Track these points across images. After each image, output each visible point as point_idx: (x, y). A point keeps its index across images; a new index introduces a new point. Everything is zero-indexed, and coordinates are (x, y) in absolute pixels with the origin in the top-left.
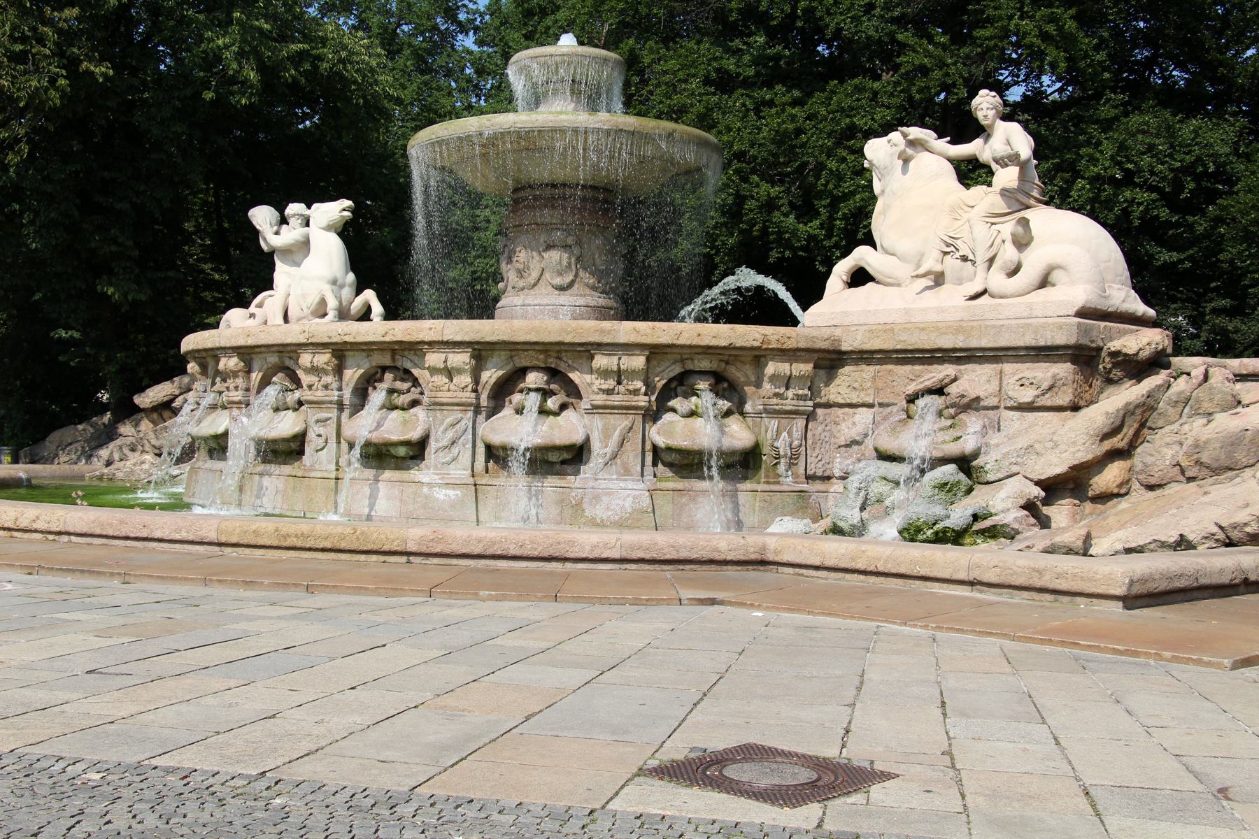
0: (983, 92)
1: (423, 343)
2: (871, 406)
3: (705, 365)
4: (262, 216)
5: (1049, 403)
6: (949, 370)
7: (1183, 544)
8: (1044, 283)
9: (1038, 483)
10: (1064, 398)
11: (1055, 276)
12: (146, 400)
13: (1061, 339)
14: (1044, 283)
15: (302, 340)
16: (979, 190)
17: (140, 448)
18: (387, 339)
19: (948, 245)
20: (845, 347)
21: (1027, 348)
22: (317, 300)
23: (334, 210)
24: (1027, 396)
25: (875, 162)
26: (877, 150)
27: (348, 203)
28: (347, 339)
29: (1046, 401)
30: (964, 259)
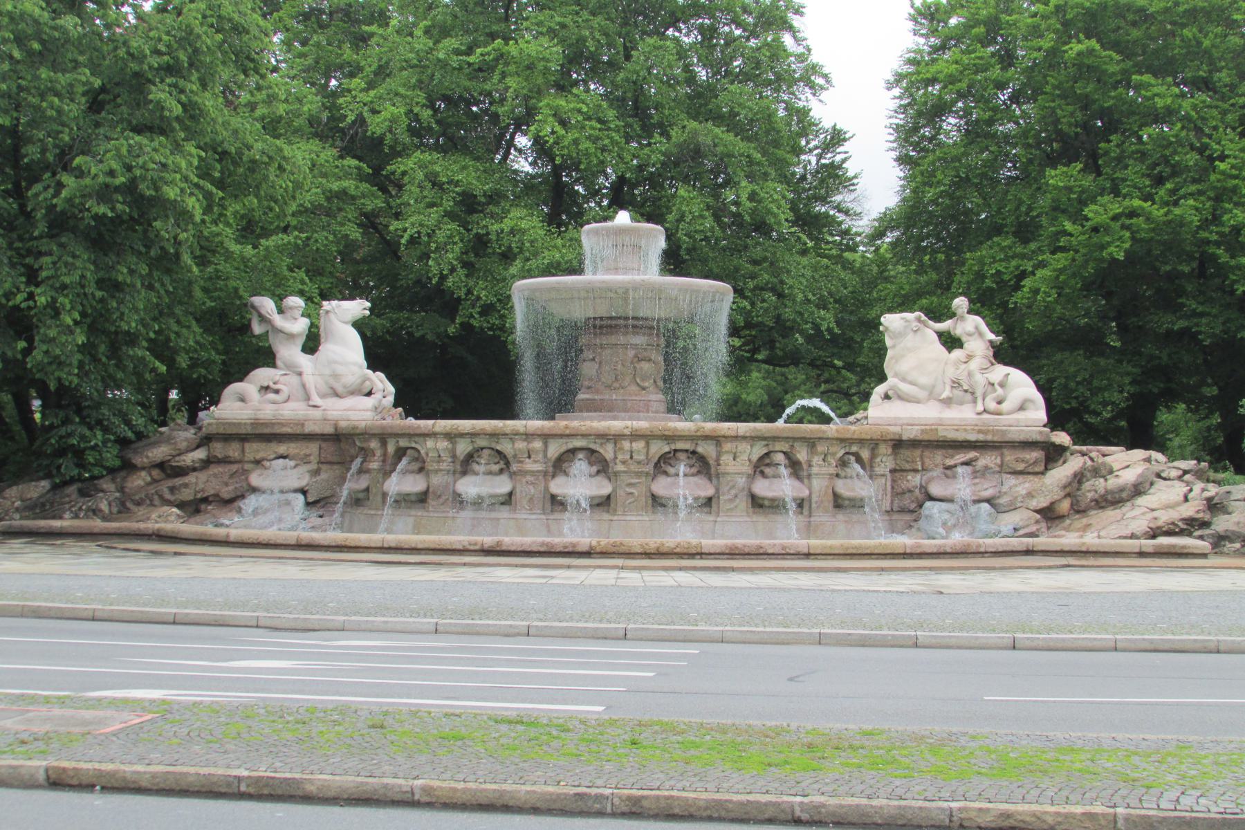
0: (962, 298)
1: (724, 437)
2: (916, 471)
3: (854, 449)
4: (266, 304)
5: (1031, 471)
6: (972, 454)
7: (1133, 536)
8: (1022, 408)
9: (1037, 511)
10: (1037, 469)
11: (1028, 404)
12: (145, 460)
13: (1039, 438)
14: (1022, 408)
15: (627, 432)
16: (957, 353)
17: (148, 502)
18: (699, 434)
19: (954, 382)
20: (905, 438)
21: (1020, 442)
22: (359, 381)
23: (358, 307)
24: (1021, 467)
25: (891, 328)
26: (892, 321)
27: (368, 304)
28: (666, 433)
29: (1030, 469)
30: (966, 391)
